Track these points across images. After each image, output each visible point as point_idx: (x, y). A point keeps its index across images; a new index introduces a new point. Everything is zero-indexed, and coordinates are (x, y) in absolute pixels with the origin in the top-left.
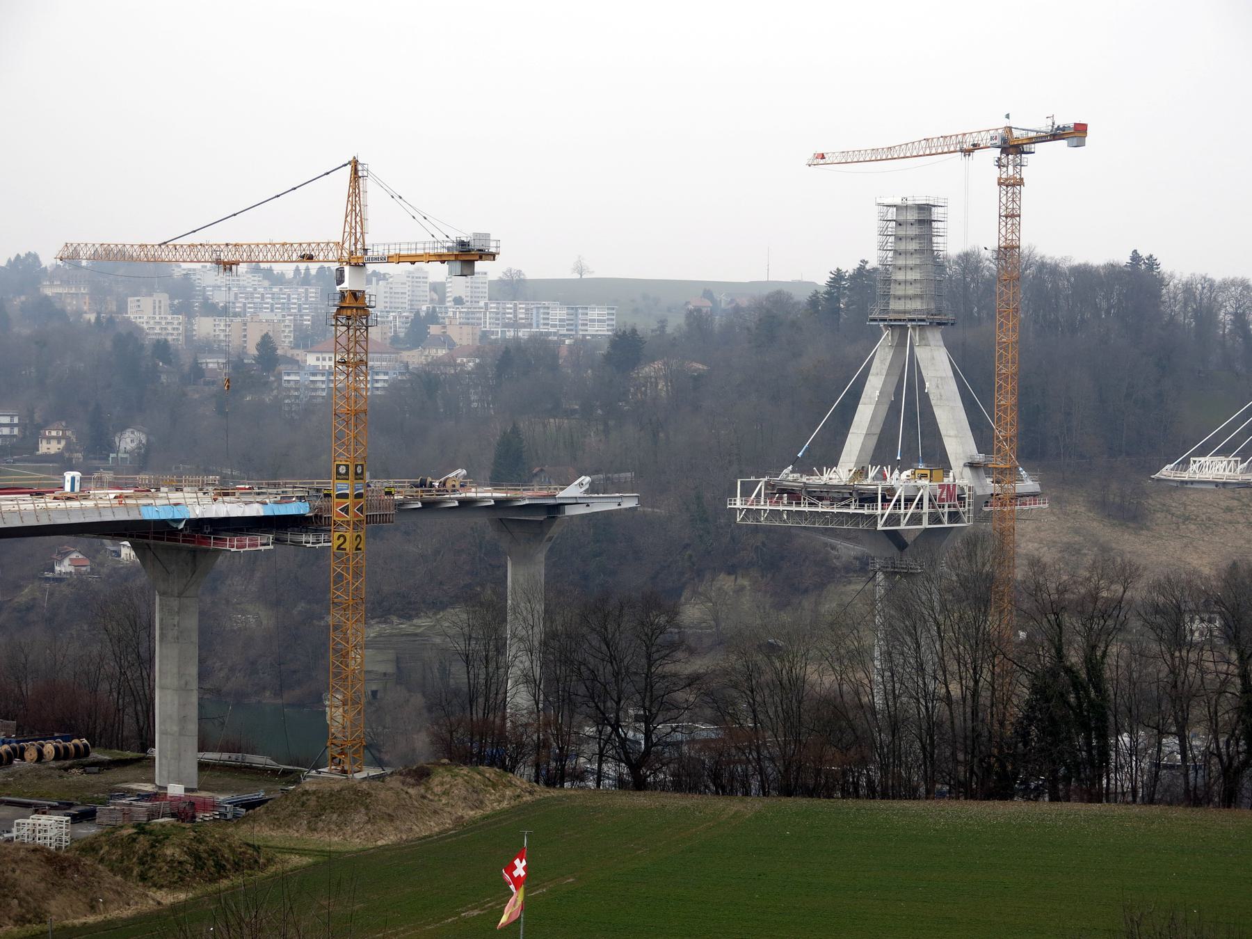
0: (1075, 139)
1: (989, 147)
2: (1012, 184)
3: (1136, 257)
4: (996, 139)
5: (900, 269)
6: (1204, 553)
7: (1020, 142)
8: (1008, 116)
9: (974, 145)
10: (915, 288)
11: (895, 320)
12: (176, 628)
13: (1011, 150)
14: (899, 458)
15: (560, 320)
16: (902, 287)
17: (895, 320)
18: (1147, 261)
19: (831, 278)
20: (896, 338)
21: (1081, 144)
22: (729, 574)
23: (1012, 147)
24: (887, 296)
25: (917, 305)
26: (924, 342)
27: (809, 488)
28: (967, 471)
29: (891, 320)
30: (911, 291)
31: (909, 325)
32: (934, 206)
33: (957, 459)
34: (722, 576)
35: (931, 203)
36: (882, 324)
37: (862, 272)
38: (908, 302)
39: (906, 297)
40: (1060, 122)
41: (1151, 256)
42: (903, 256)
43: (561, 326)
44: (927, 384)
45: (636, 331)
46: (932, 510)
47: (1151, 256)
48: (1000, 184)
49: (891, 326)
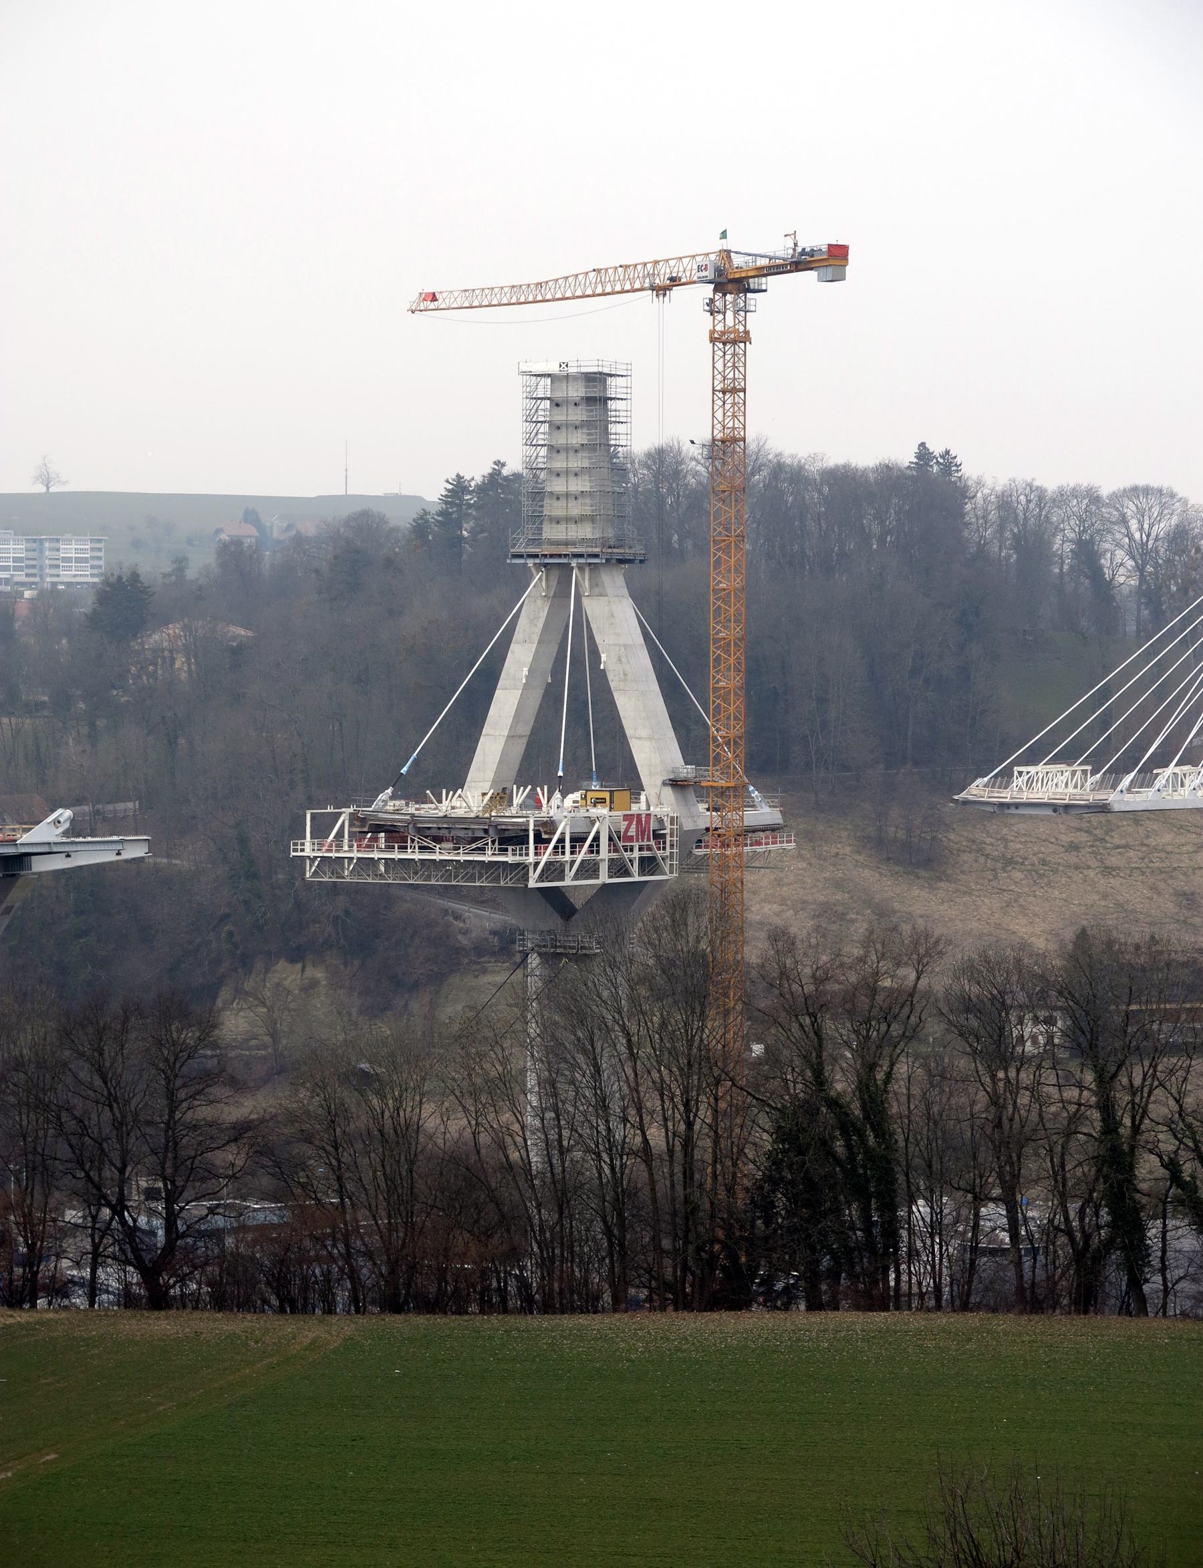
0: (830, 270)
1: (694, 282)
3: (924, 453)
4: (706, 269)
5: (558, 475)
6: (1036, 915)
7: (743, 275)
8: (724, 235)
9: (672, 279)
10: (585, 505)
11: (552, 556)
13: (730, 287)
14: (560, 773)
15: (15, 560)
16: (563, 502)
17: (552, 556)
18: (941, 461)
19: (449, 491)
20: (554, 583)
21: (839, 277)
22: (293, 961)
24: (538, 519)
25: (586, 531)
26: (596, 591)
27: (421, 822)
28: (668, 792)
29: (545, 556)
30: (576, 509)
31: (574, 563)
32: (611, 375)
33: (651, 774)
34: (282, 965)
35: (606, 370)
36: (530, 562)
37: (496, 480)
38: (572, 526)
39: (568, 519)
40: (806, 243)
41: (947, 452)
42: (562, 456)
43: (16, 569)
44: (604, 657)
45: (138, 576)
46: (614, 855)
47: (947, 452)
48: (713, 340)
49: (545, 565)
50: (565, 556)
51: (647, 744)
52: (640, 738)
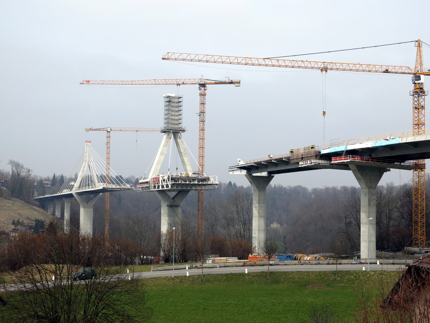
2: (203, 95)
11: (175, 130)
12: (374, 200)
17: (175, 130)
23: (203, 85)
29: (174, 130)
48: (201, 95)
50: (178, 130)
51: (190, 166)
52: (188, 165)
